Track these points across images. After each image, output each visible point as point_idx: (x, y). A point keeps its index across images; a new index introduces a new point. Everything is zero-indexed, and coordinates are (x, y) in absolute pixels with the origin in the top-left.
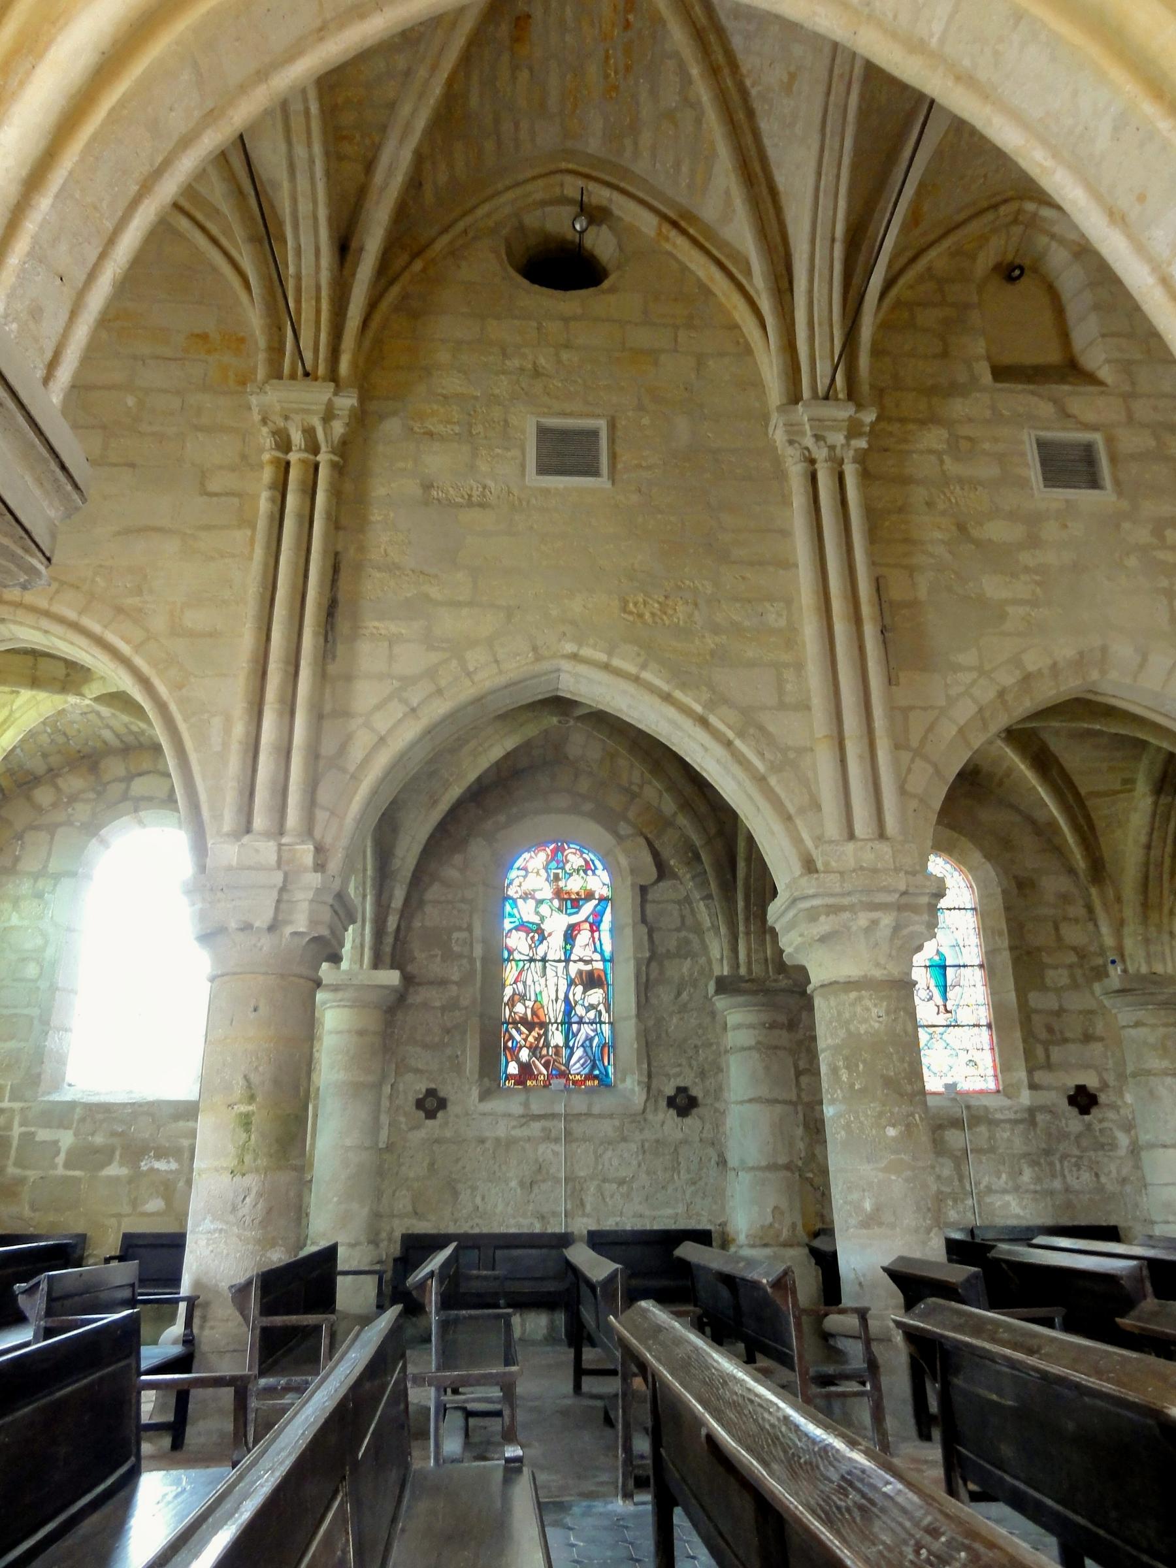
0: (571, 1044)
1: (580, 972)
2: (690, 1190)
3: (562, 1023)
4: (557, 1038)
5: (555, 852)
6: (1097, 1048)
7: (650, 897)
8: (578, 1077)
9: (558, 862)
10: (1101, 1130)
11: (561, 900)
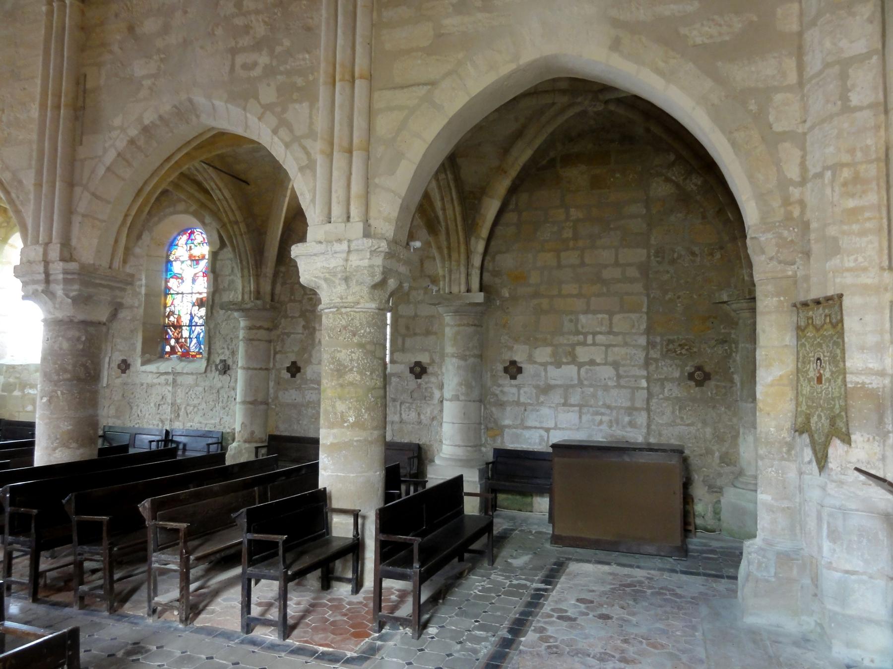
0: (191, 336)
1: (197, 299)
2: (222, 412)
3: (188, 326)
4: (185, 333)
5: (190, 234)
6: (432, 338)
7: (219, 257)
8: (194, 353)
9: (192, 240)
10: (426, 389)
11: (192, 260)
